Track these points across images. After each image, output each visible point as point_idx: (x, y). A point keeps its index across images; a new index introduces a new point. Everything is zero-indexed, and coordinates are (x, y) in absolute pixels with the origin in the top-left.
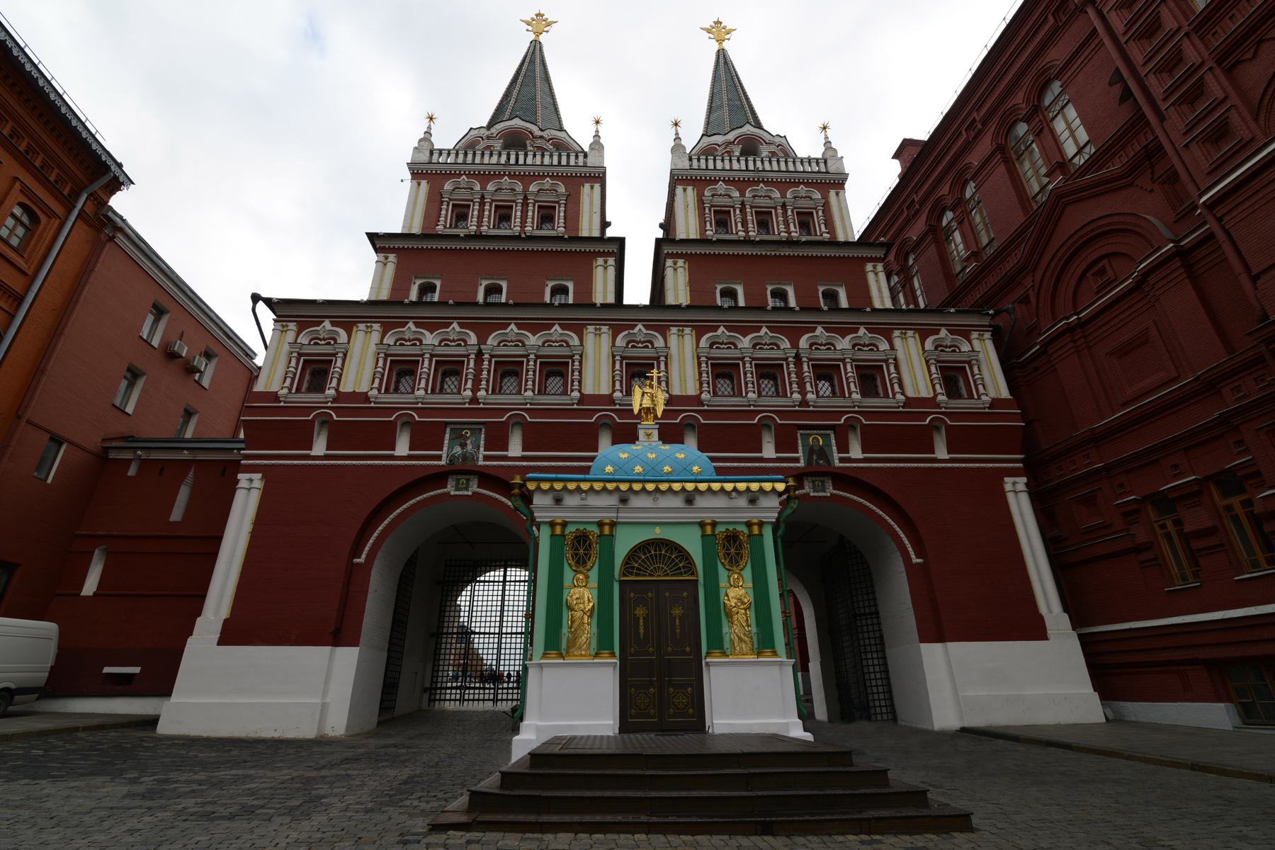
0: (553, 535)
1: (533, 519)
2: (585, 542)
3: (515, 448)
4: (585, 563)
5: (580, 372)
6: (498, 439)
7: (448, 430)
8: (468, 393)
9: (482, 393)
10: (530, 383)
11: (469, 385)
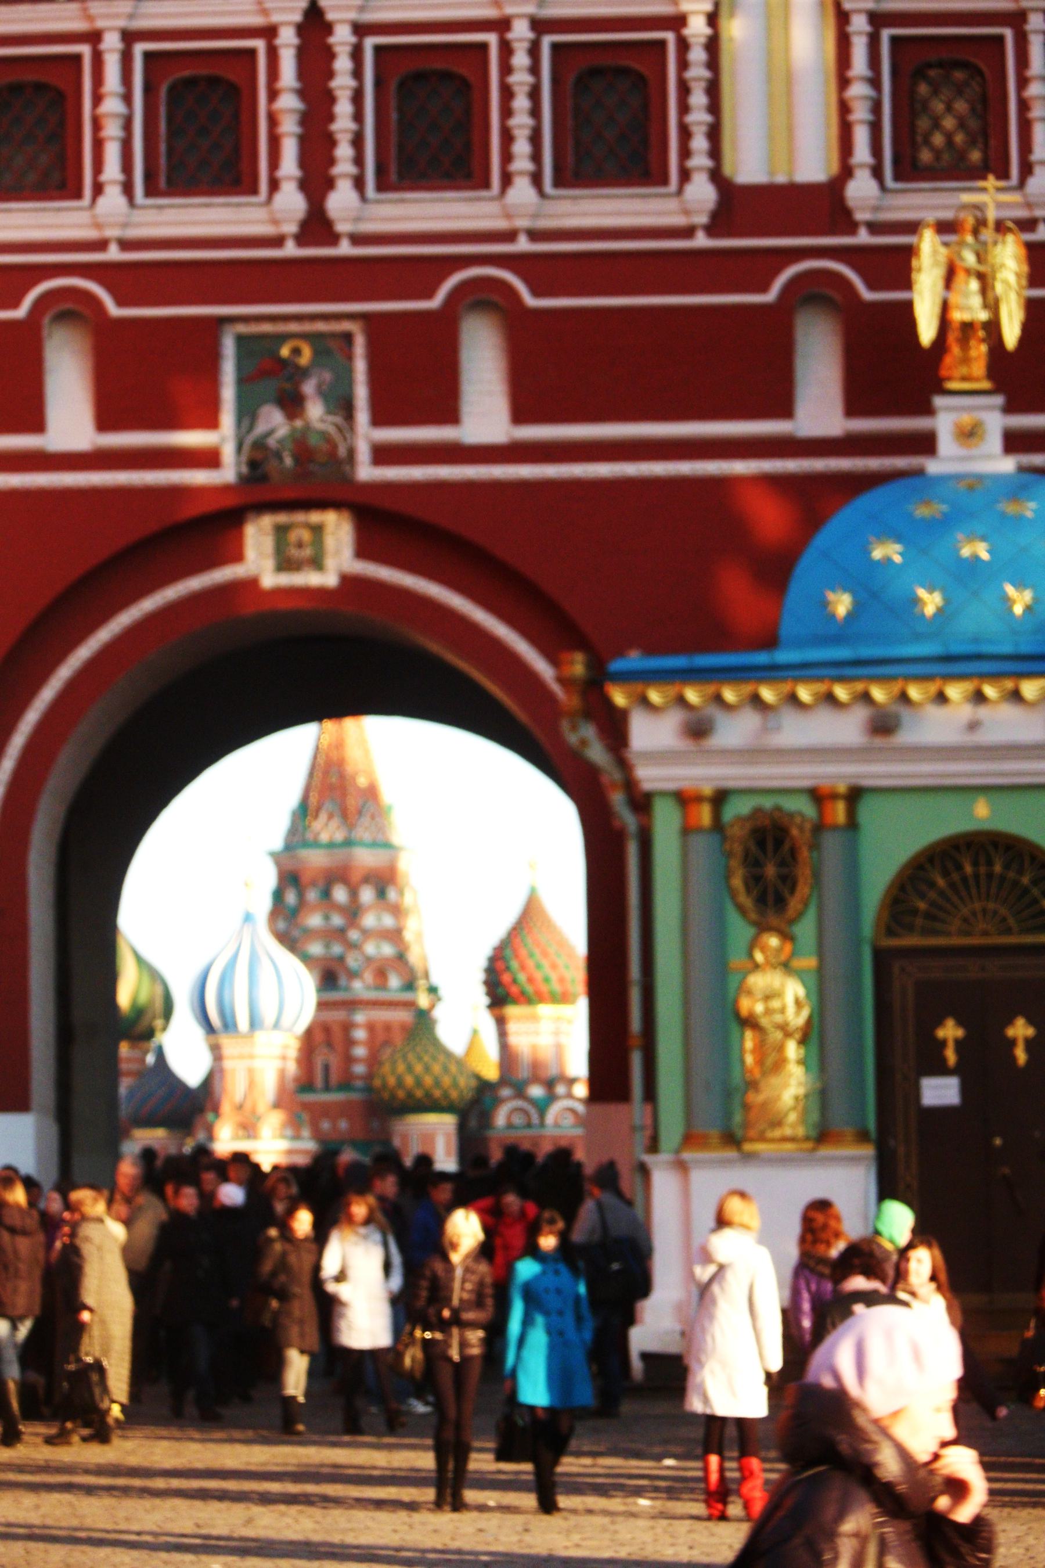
0: (687, 830)
1: (630, 785)
2: (779, 843)
3: (485, 412)
4: (780, 903)
5: (713, 90)
6: (417, 379)
7: (229, 347)
8: (291, 201)
9: (341, 201)
10: (522, 147)
11: (289, 165)
